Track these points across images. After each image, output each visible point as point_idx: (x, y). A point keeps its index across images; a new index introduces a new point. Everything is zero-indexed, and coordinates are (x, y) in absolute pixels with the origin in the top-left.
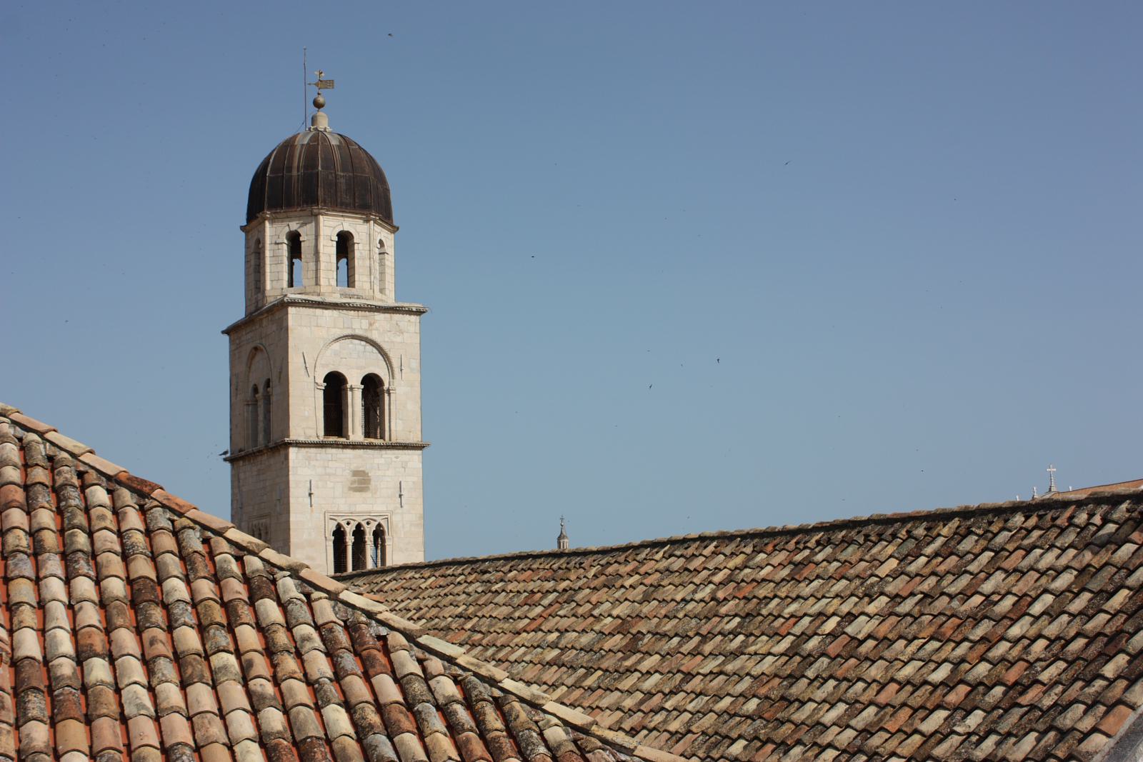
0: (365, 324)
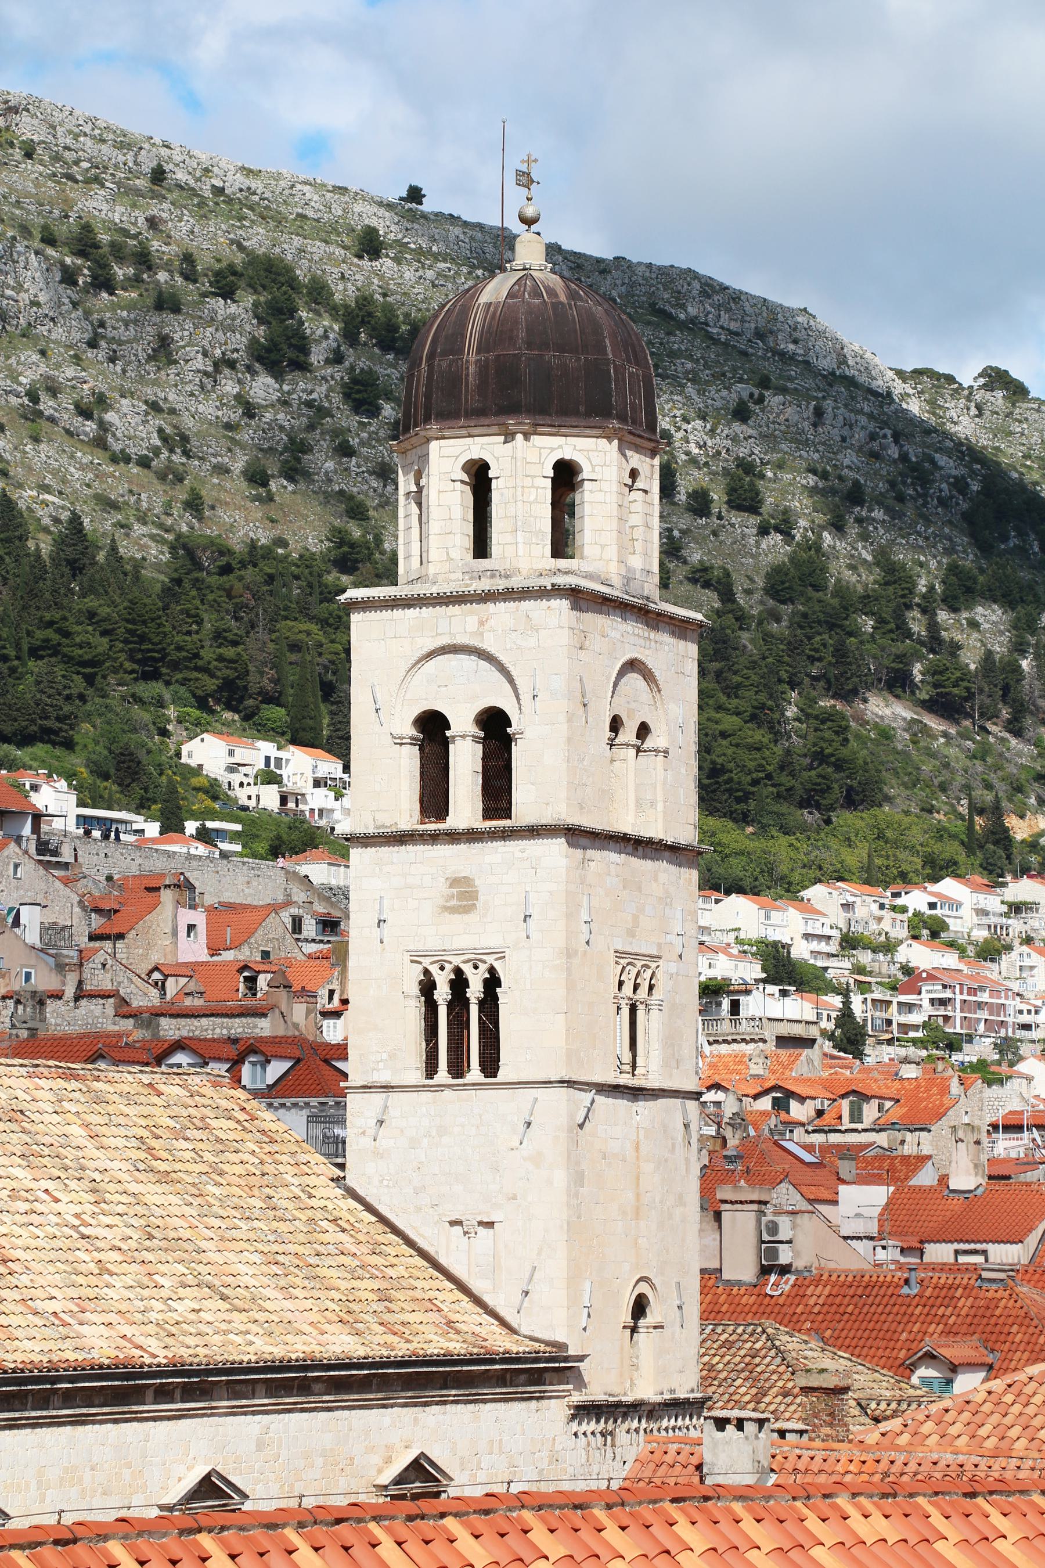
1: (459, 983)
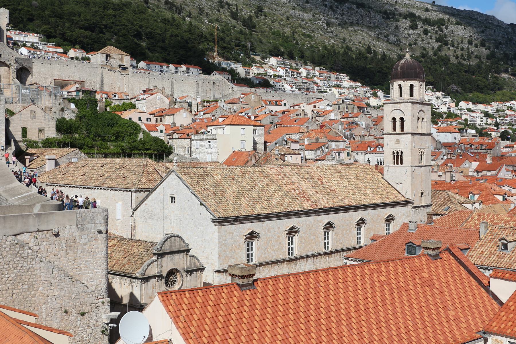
1: (398, 153)
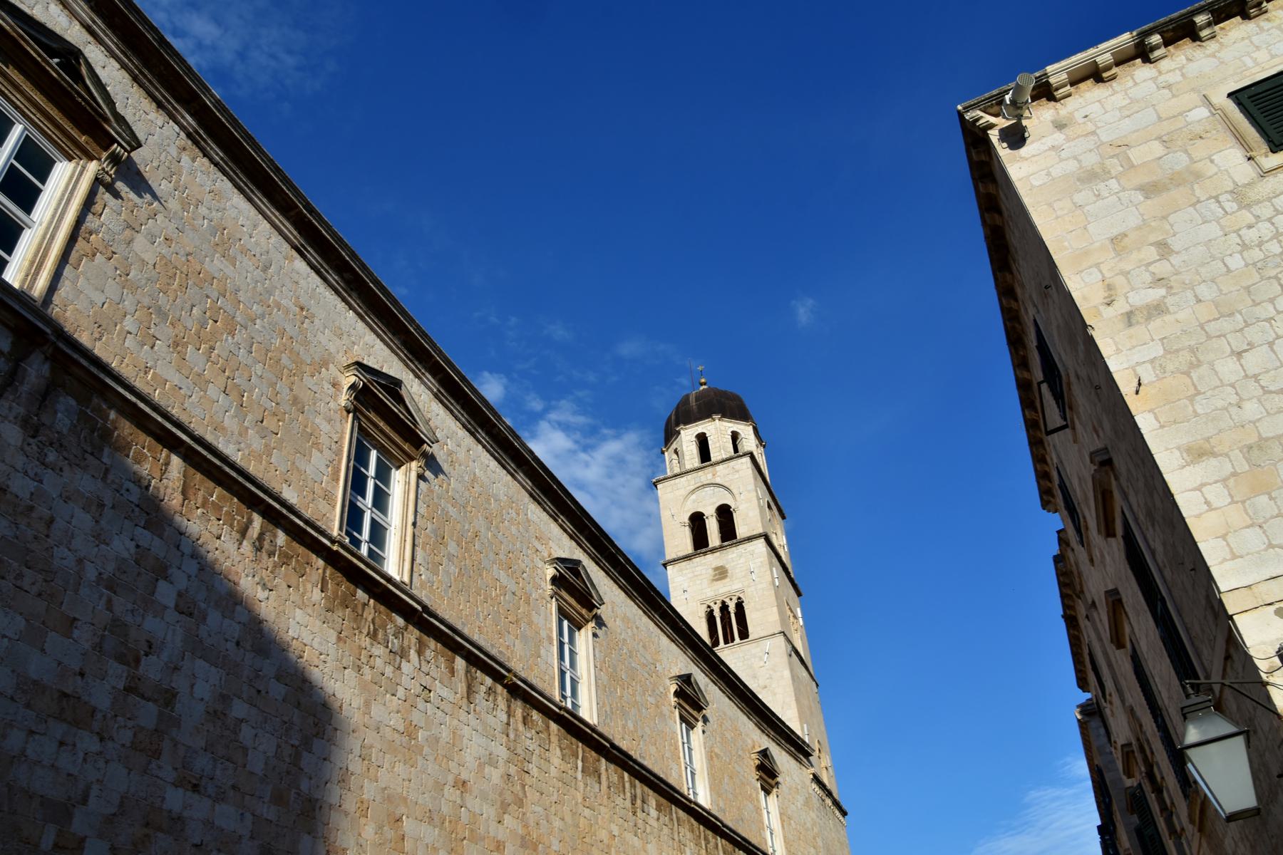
0: (710, 476)
1: (724, 608)
